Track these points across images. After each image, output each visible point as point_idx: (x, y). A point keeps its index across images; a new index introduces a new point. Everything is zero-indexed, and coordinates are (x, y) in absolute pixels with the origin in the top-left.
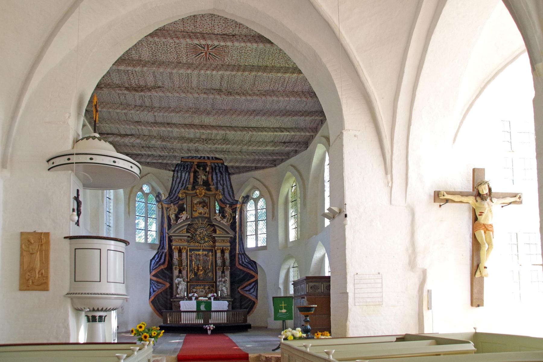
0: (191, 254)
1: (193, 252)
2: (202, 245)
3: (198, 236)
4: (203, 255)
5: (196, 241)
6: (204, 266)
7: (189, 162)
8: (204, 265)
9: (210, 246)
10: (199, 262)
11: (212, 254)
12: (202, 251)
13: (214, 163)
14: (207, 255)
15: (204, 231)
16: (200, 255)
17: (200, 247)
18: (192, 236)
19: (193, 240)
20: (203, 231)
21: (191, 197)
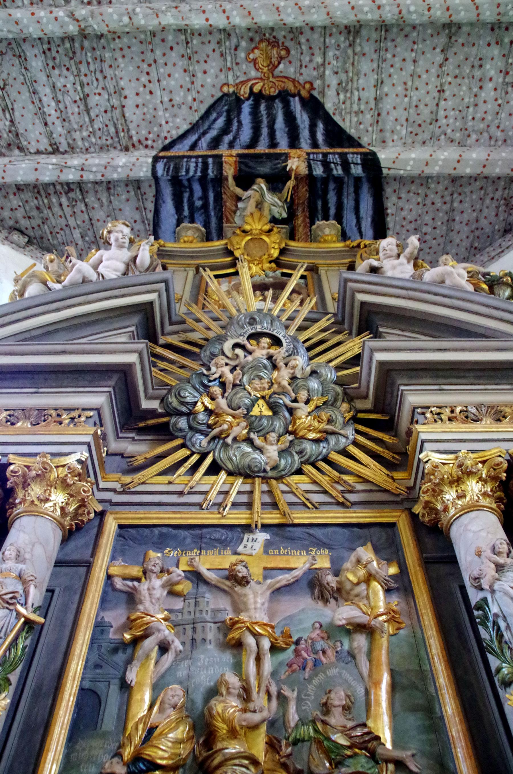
0: (136, 571)
1: (154, 555)
2: (270, 493)
3: (223, 402)
4: (284, 578)
5: (204, 456)
6: (293, 717)
7: (197, 157)
8: (291, 694)
9: (353, 498)
10: (228, 657)
11: (393, 570)
12: (268, 545)
13: (325, 155)
14: (331, 580)
15: (279, 353)
16: (243, 582)
17: (249, 505)
18: (163, 400)
19: (179, 442)
20: (270, 358)
21: (191, 273)
